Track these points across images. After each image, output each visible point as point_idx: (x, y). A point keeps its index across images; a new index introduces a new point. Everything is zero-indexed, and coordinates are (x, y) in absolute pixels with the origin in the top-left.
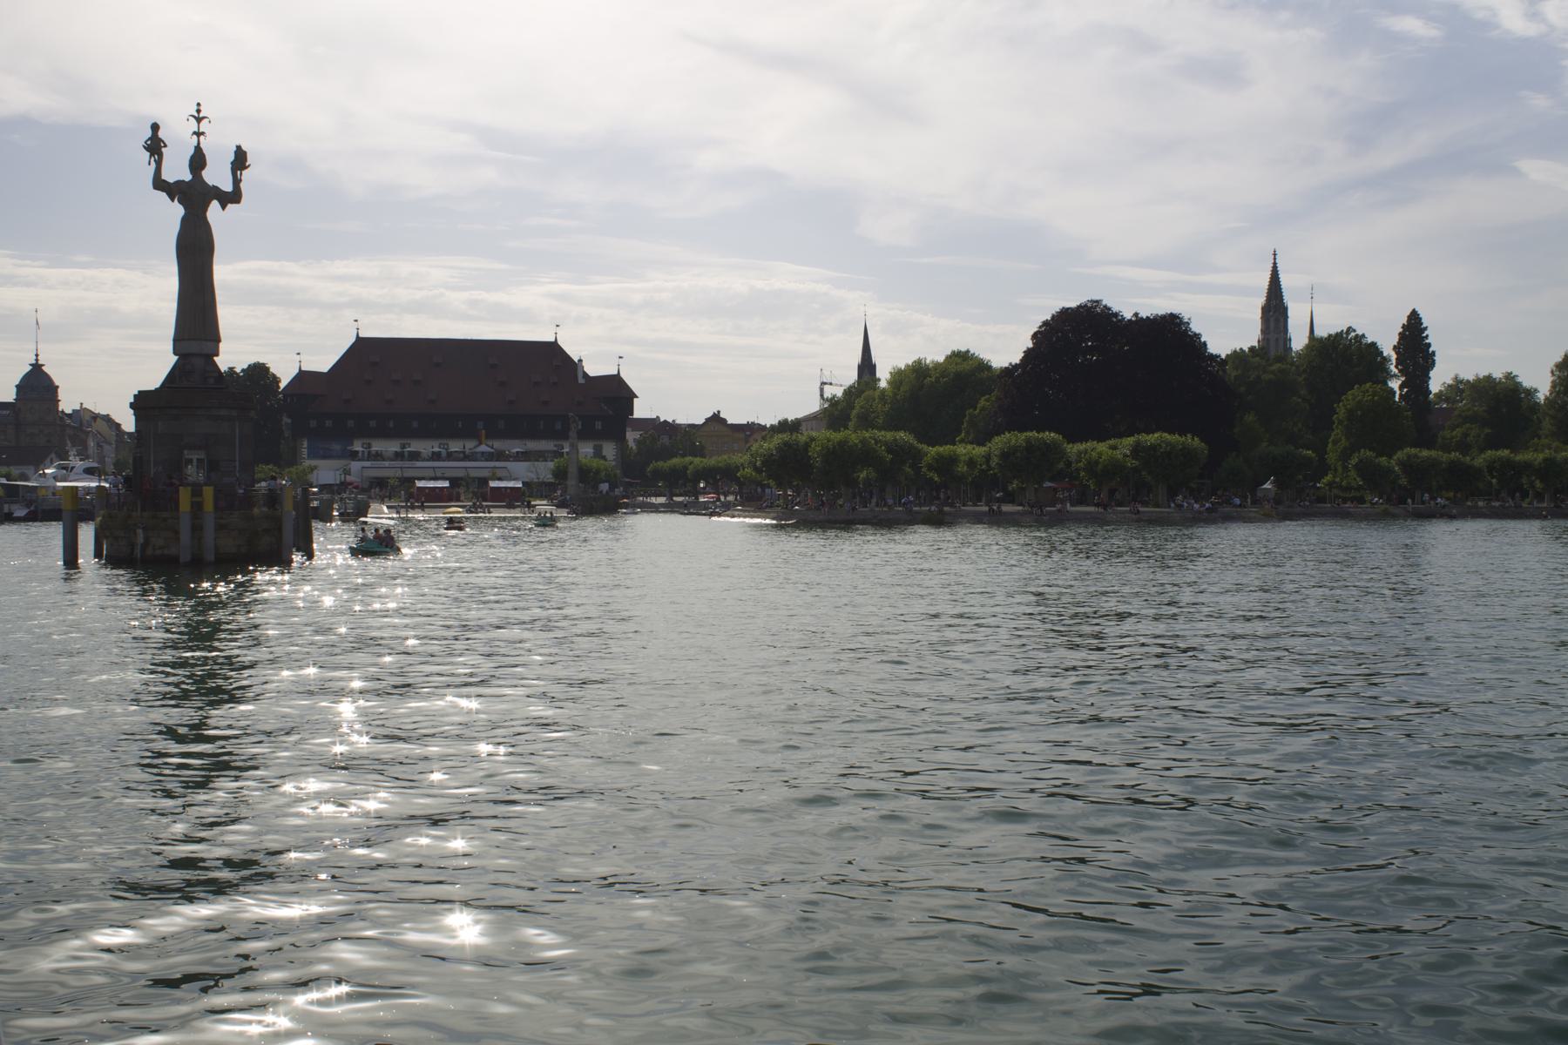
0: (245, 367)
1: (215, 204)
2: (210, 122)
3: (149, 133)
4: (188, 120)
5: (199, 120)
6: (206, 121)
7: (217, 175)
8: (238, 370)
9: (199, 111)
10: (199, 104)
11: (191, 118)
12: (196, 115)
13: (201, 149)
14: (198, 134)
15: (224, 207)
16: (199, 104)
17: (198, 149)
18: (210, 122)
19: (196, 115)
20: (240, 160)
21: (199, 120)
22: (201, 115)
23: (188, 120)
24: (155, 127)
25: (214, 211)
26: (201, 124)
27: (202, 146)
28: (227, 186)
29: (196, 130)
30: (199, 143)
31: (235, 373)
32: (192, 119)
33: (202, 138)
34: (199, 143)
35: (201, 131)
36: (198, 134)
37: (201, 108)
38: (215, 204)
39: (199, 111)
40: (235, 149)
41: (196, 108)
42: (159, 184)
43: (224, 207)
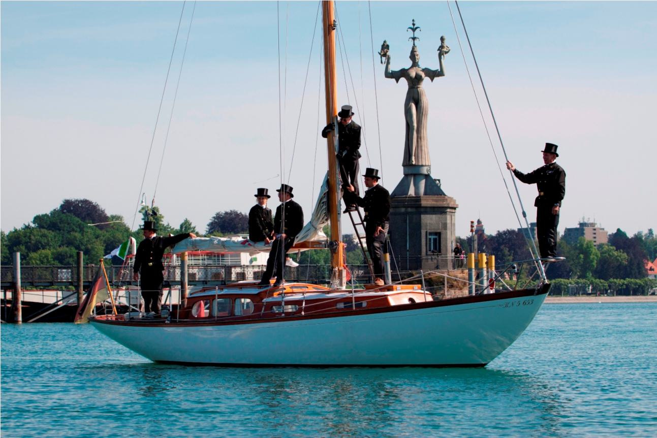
1: (426, 80)
5: (414, 30)
6: (418, 30)
7: (427, 60)
9: (414, 25)
10: (413, 20)
11: (409, 30)
12: (412, 27)
14: (414, 39)
15: (432, 80)
16: (413, 20)
19: (412, 27)
20: (442, 51)
21: (414, 30)
22: (415, 27)
25: (426, 85)
28: (435, 67)
29: (413, 36)
30: (414, 44)
32: (410, 30)
33: (416, 41)
34: (414, 44)
36: (414, 39)
37: (415, 23)
38: (426, 80)
39: (414, 25)
41: (412, 22)
42: (390, 75)
43: (432, 80)
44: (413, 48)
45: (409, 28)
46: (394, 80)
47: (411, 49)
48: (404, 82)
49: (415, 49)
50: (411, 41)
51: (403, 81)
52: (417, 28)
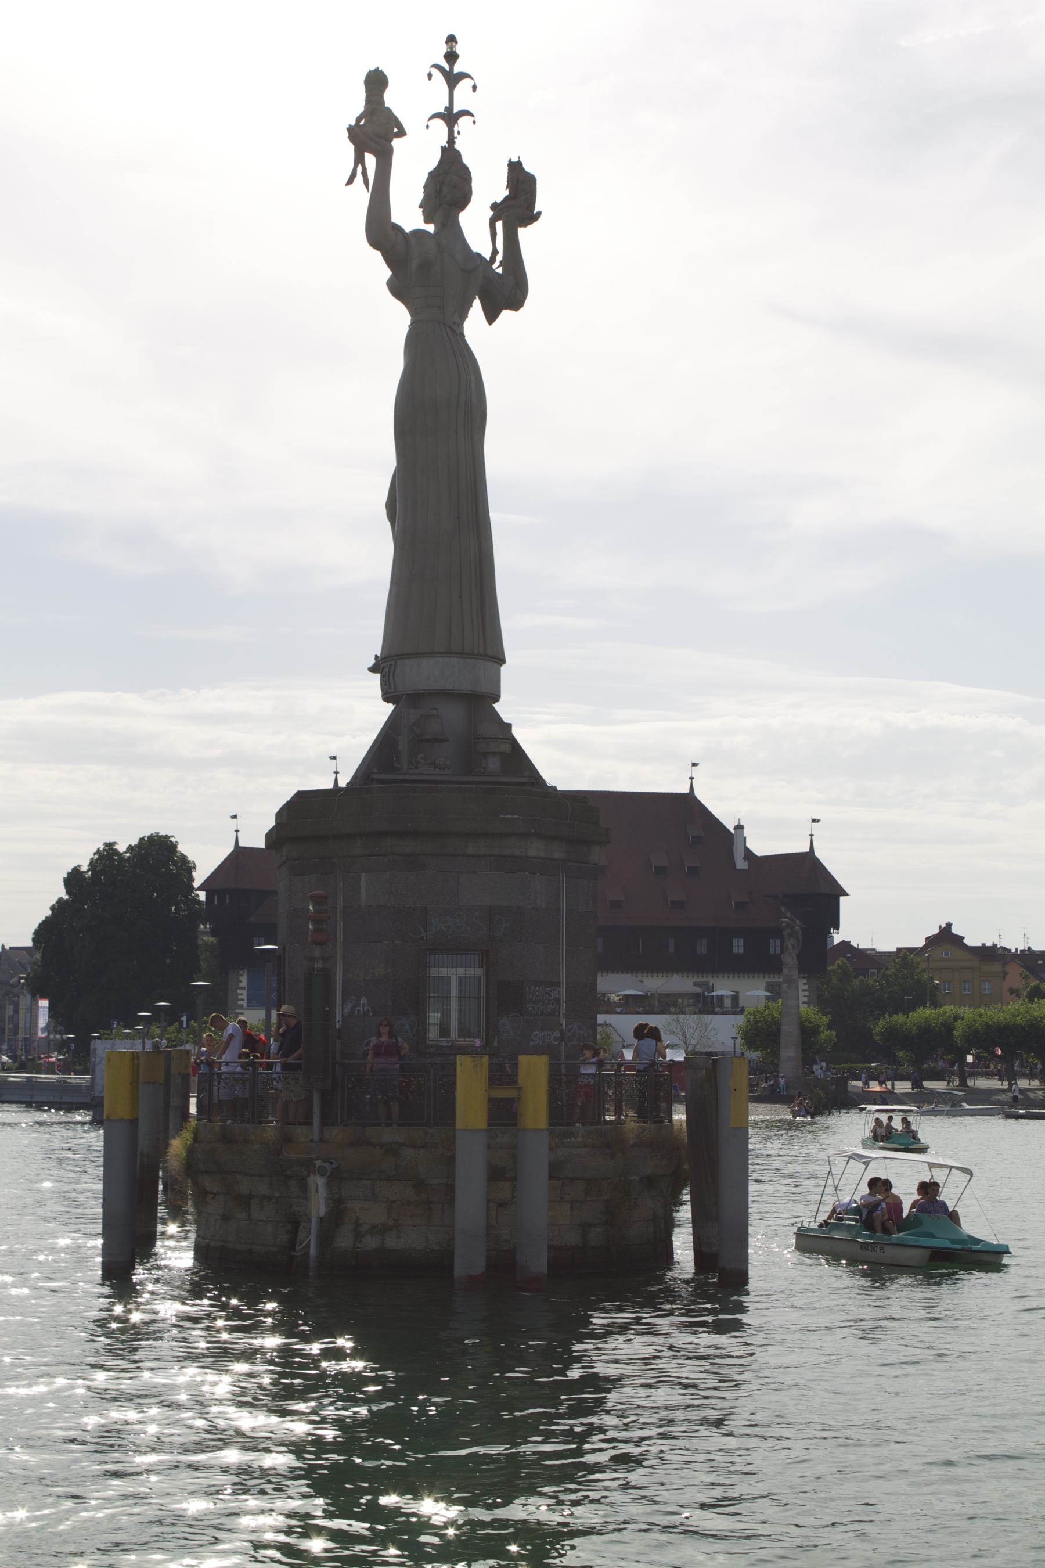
0: (134, 842)
2: (474, 88)
4: (430, 76)
5: (453, 79)
8: (121, 848)
9: (451, 57)
10: (451, 39)
11: (436, 73)
13: (458, 155)
14: (450, 117)
16: (451, 39)
17: (450, 156)
18: (474, 88)
22: (458, 68)
23: (430, 76)
26: (457, 91)
27: (458, 146)
30: (451, 140)
31: (116, 852)
33: (463, 122)
34: (451, 140)
35: (456, 110)
36: (450, 117)
37: (459, 49)
39: (451, 57)
41: (444, 49)
50: (441, 126)
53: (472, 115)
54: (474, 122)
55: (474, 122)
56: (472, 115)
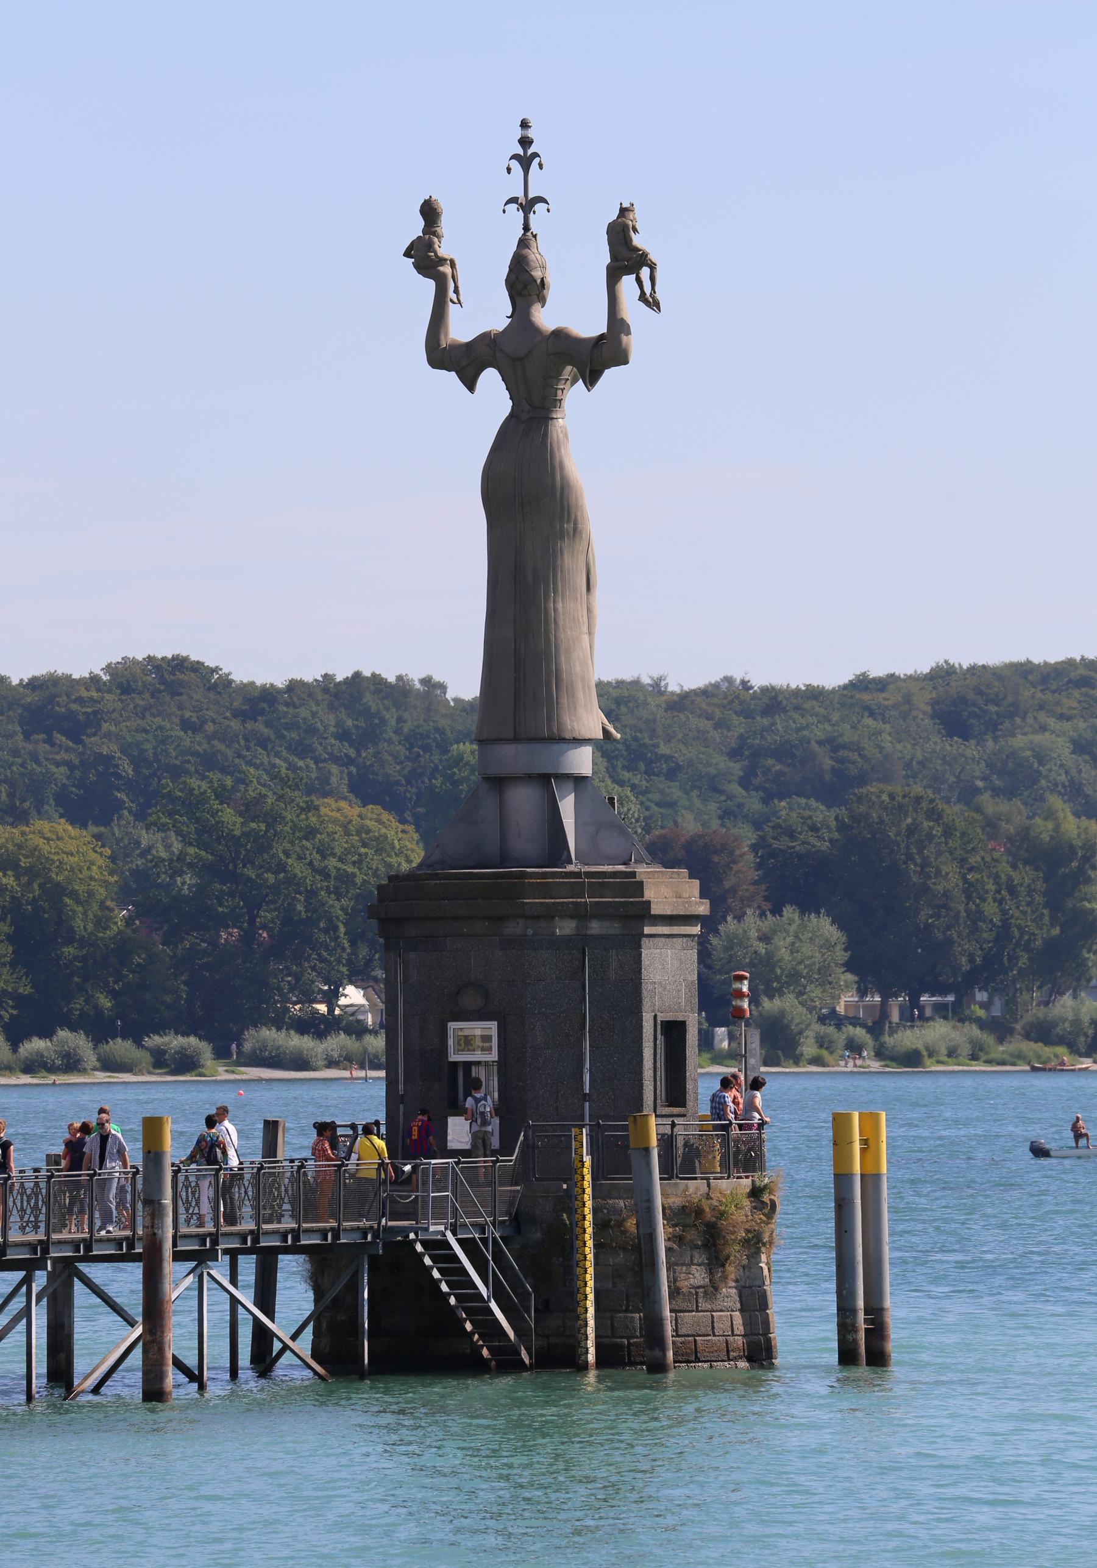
3: (416, 227)
5: (526, 162)
9: (525, 142)
10: (525, 125)
16: (525, 125)
21: (526, 162)
22: (530, 152)
24: (430, 212)
29: (520, 194)
30: (526, 228)
32: (515, 165)
34: (526, 228)
35: (531, 195)
36: (528, 205)
39: (525, 142)
40: (613, 215)
41: (518, 133)
44: (523, 243)
45: (515, 157)
46: (451, 378)
47: (513, 248)
48: (491, 379)
49: (532, 255)
50: (515, 215)
51: (491, 379)
52: (535, 155)
53: (546, 202)
54: (548, 210)
55: (548, 210)
56: (546, 202)
